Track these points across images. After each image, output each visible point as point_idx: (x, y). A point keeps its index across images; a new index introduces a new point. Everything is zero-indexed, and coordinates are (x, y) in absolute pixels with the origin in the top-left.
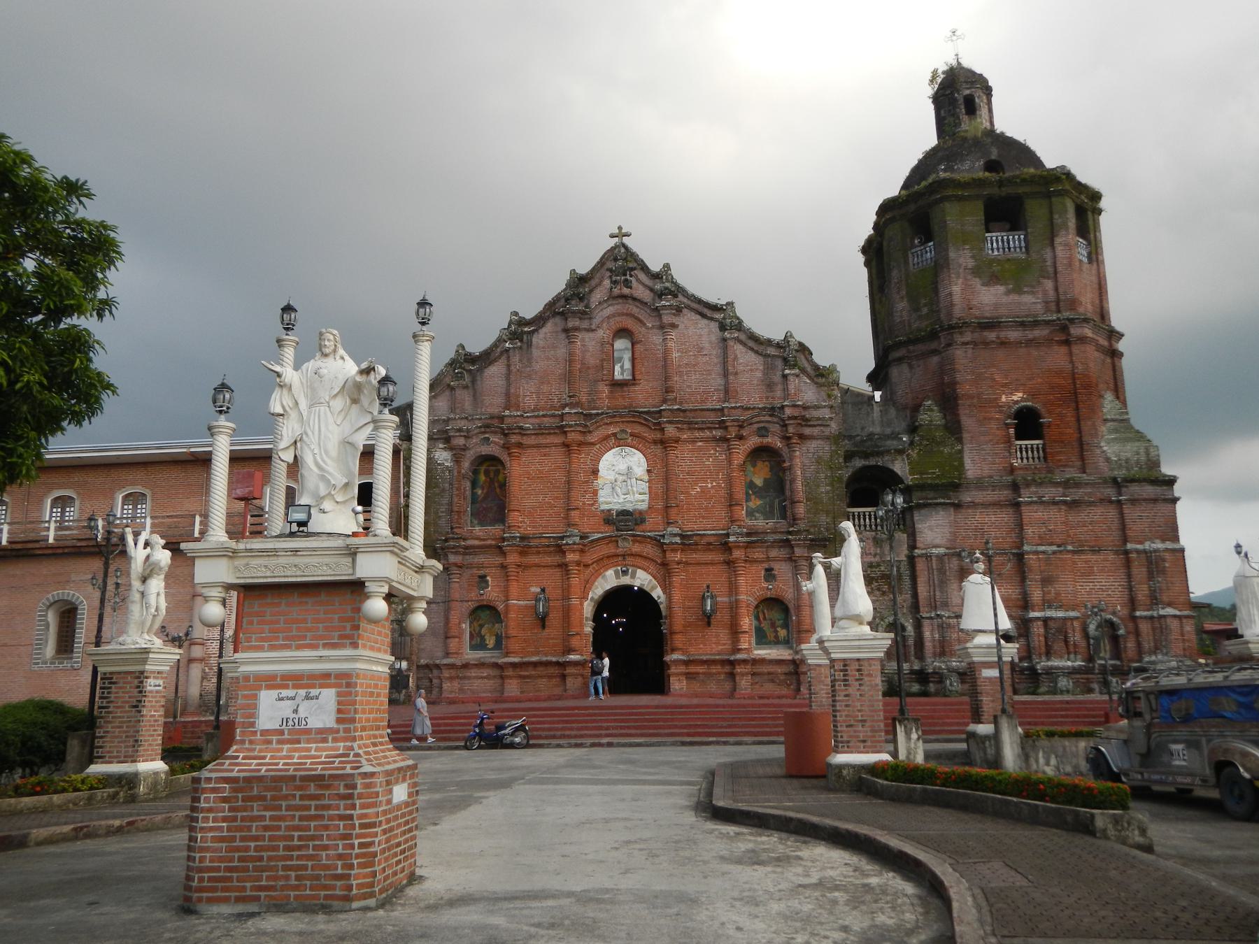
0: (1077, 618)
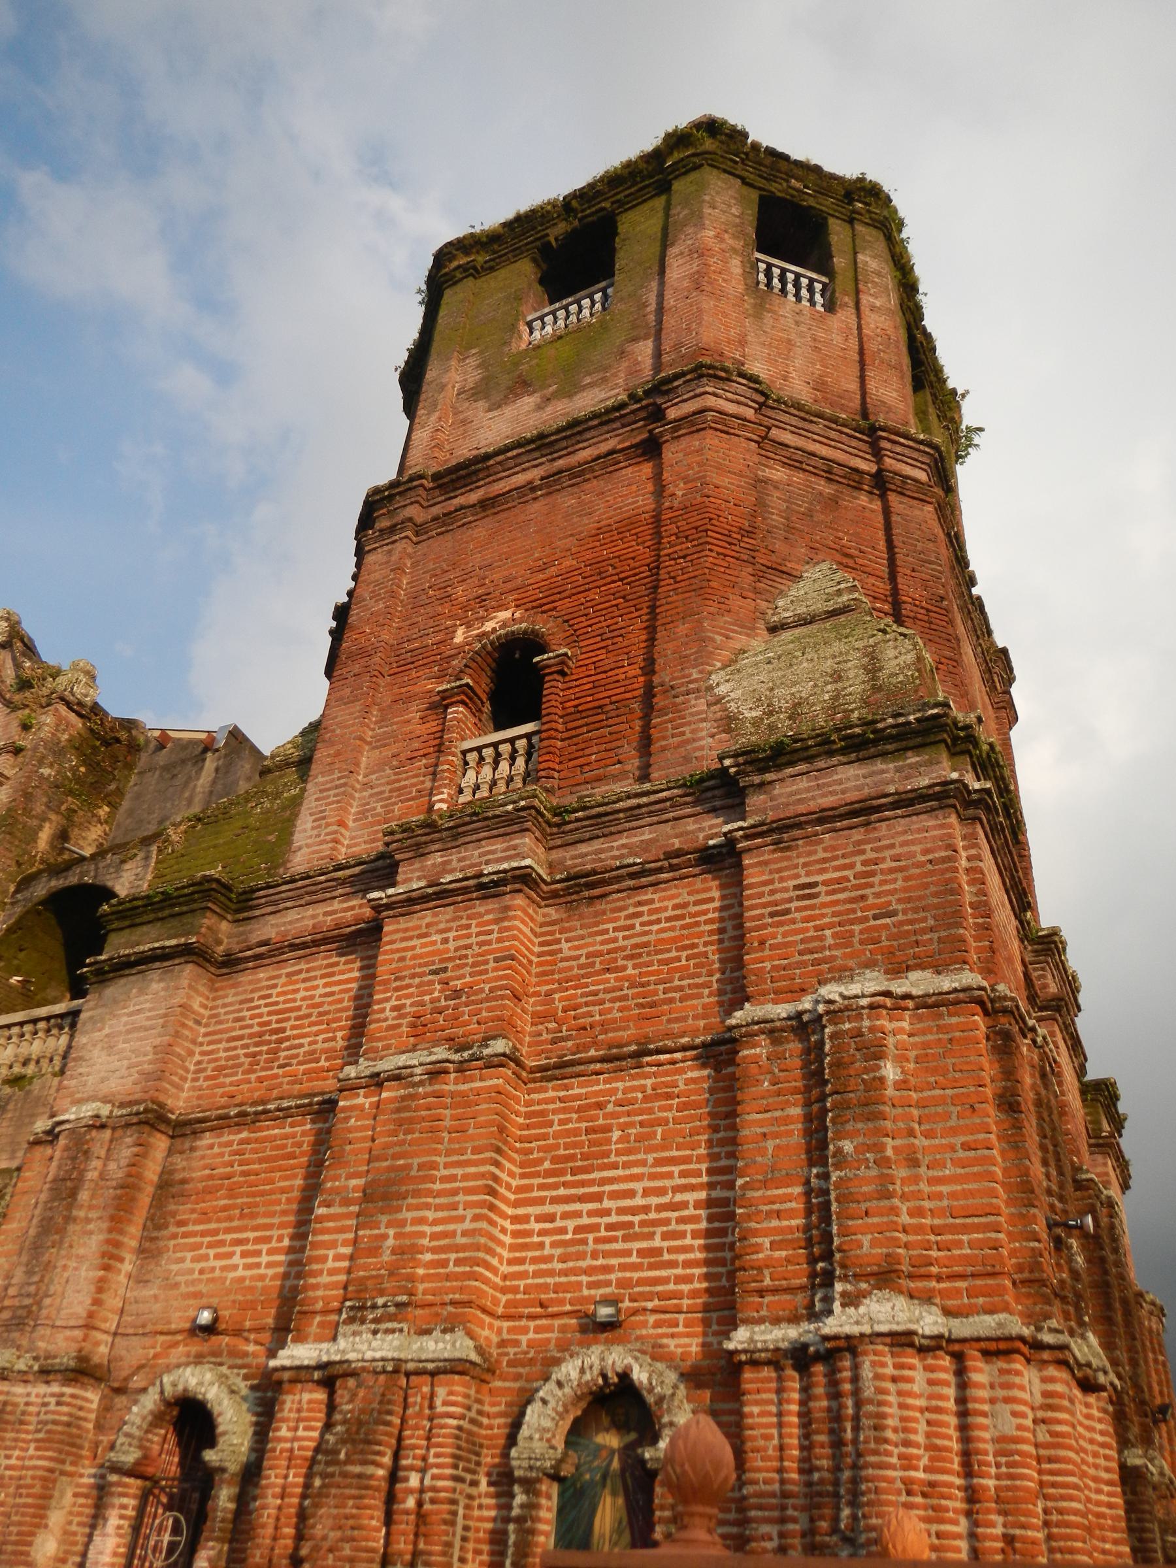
0: (455, 1368)
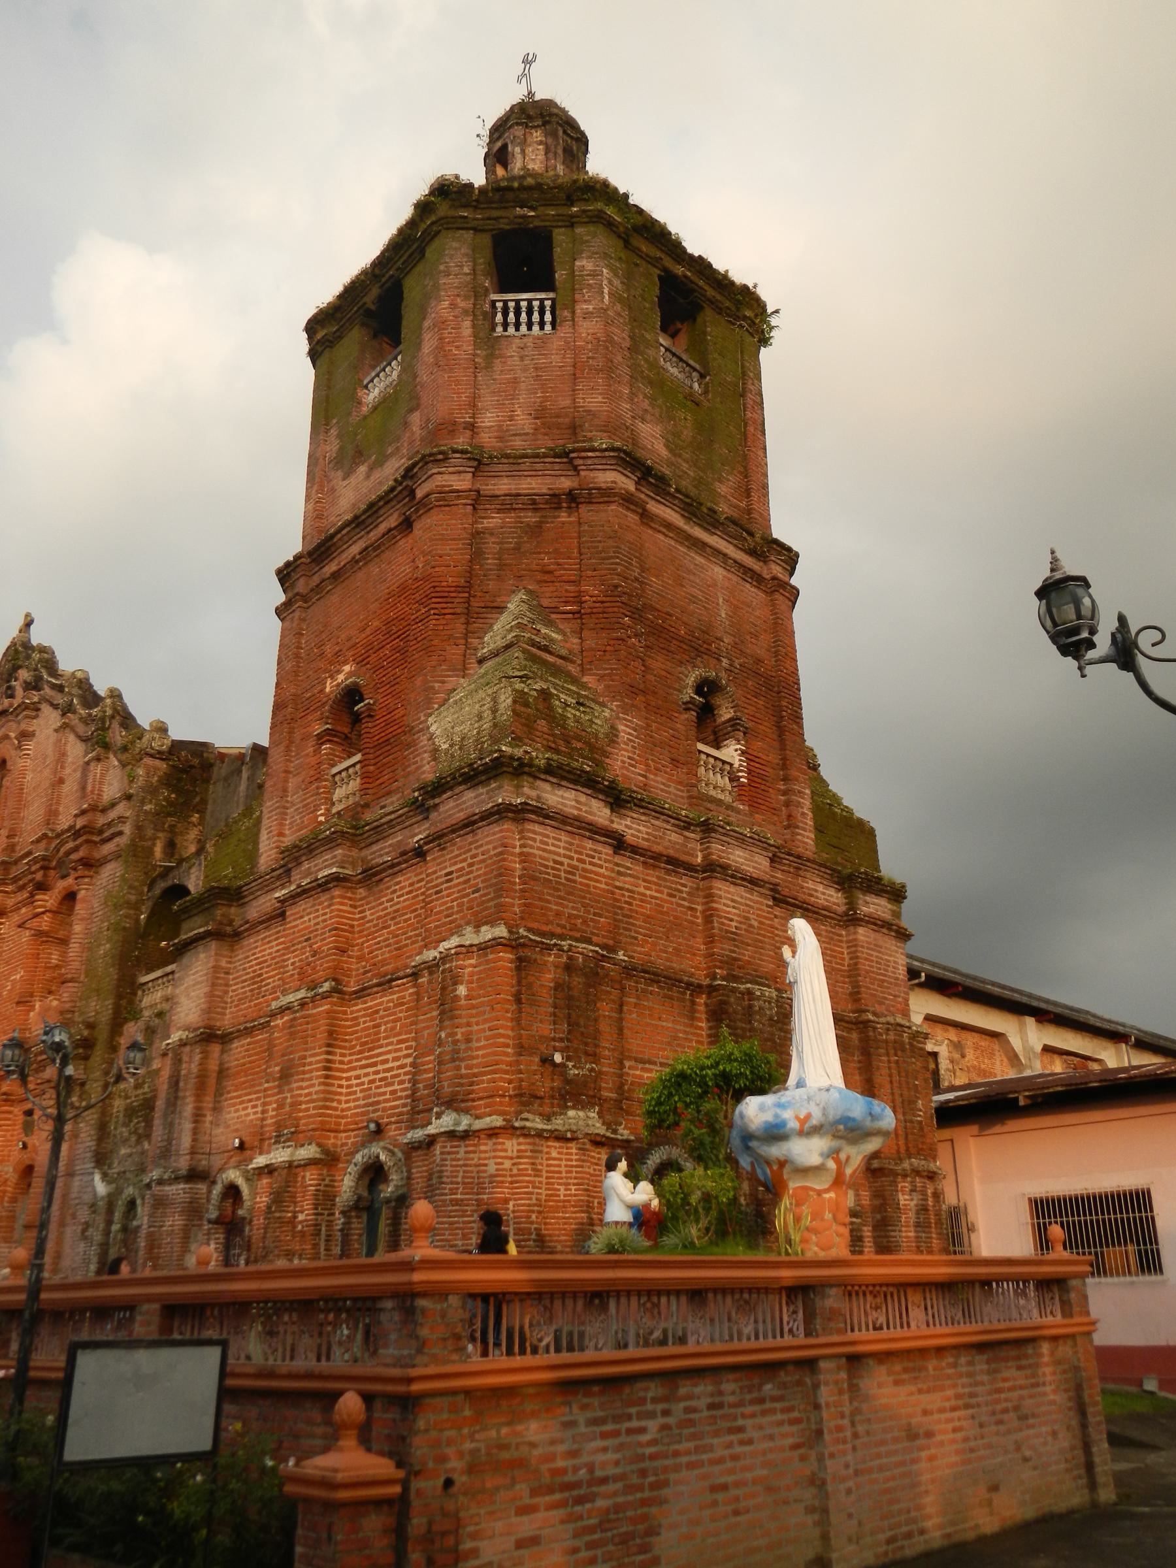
0: (312, 1162)
